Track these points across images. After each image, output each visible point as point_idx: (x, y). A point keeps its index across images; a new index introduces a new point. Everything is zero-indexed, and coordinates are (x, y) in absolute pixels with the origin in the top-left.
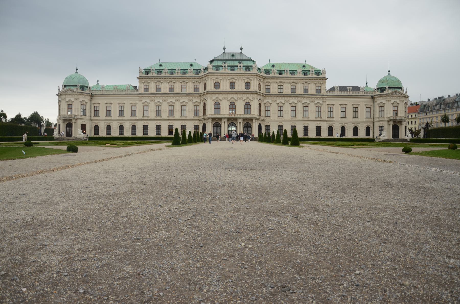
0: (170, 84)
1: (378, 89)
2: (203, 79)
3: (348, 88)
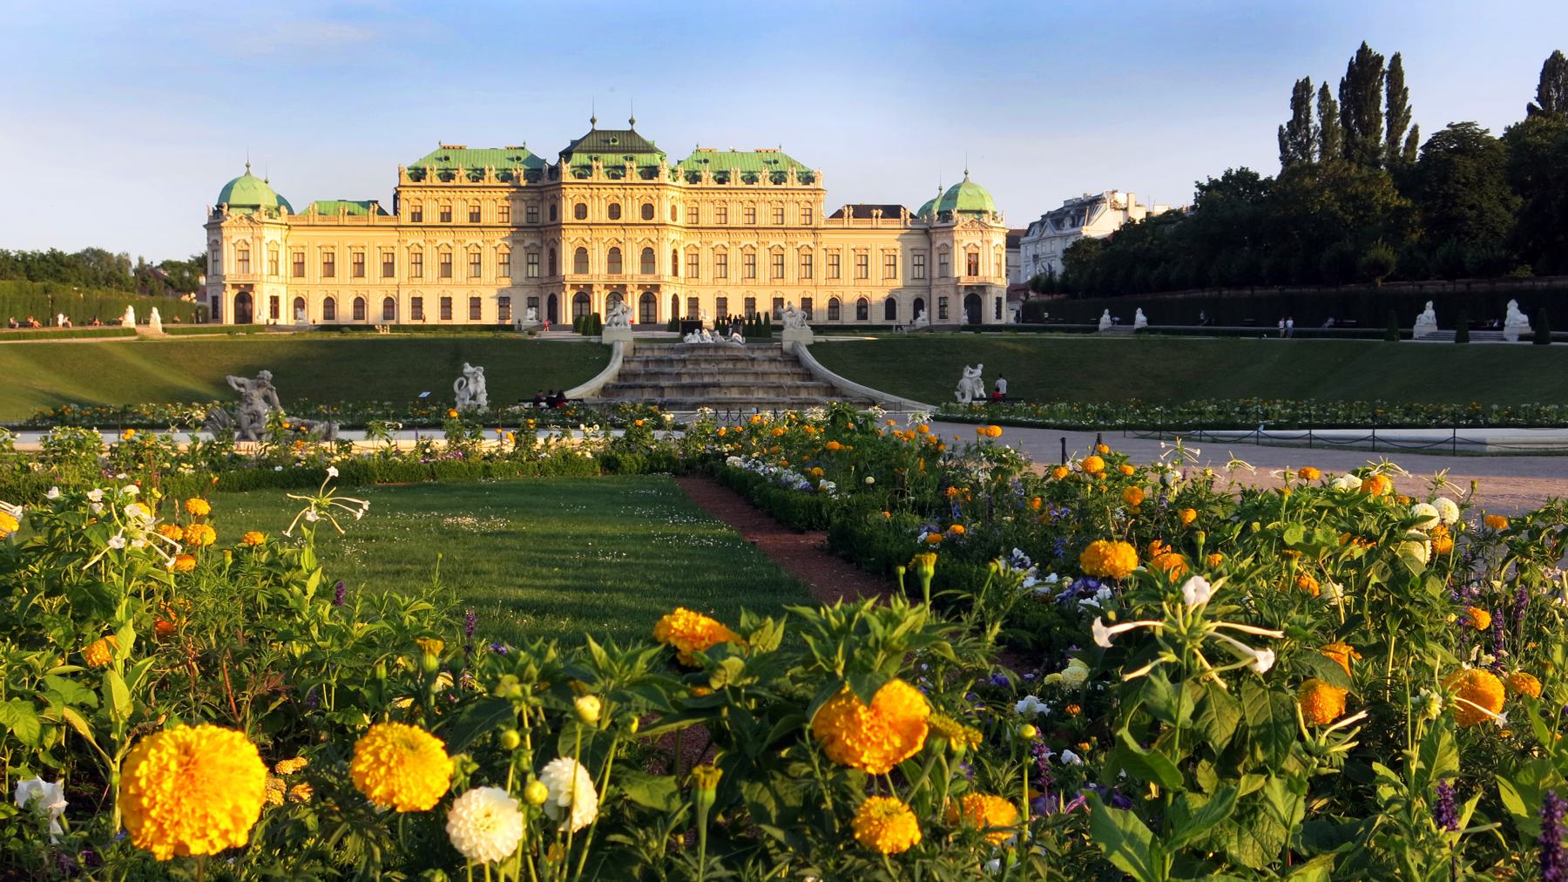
2: (548, 195)
3: (875, 212)
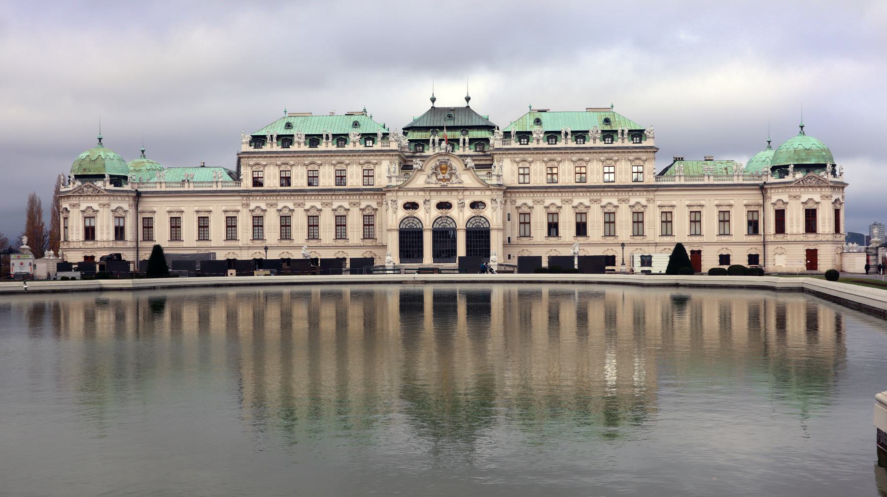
0: (310, 168)
1: (773, 169)
